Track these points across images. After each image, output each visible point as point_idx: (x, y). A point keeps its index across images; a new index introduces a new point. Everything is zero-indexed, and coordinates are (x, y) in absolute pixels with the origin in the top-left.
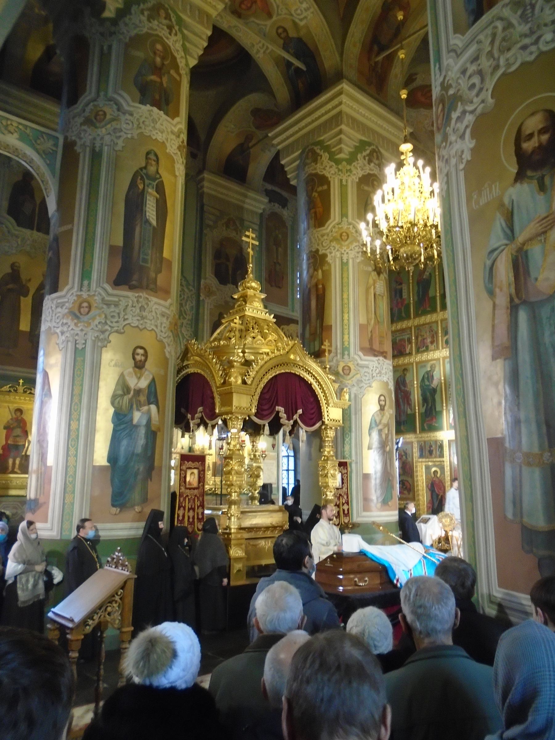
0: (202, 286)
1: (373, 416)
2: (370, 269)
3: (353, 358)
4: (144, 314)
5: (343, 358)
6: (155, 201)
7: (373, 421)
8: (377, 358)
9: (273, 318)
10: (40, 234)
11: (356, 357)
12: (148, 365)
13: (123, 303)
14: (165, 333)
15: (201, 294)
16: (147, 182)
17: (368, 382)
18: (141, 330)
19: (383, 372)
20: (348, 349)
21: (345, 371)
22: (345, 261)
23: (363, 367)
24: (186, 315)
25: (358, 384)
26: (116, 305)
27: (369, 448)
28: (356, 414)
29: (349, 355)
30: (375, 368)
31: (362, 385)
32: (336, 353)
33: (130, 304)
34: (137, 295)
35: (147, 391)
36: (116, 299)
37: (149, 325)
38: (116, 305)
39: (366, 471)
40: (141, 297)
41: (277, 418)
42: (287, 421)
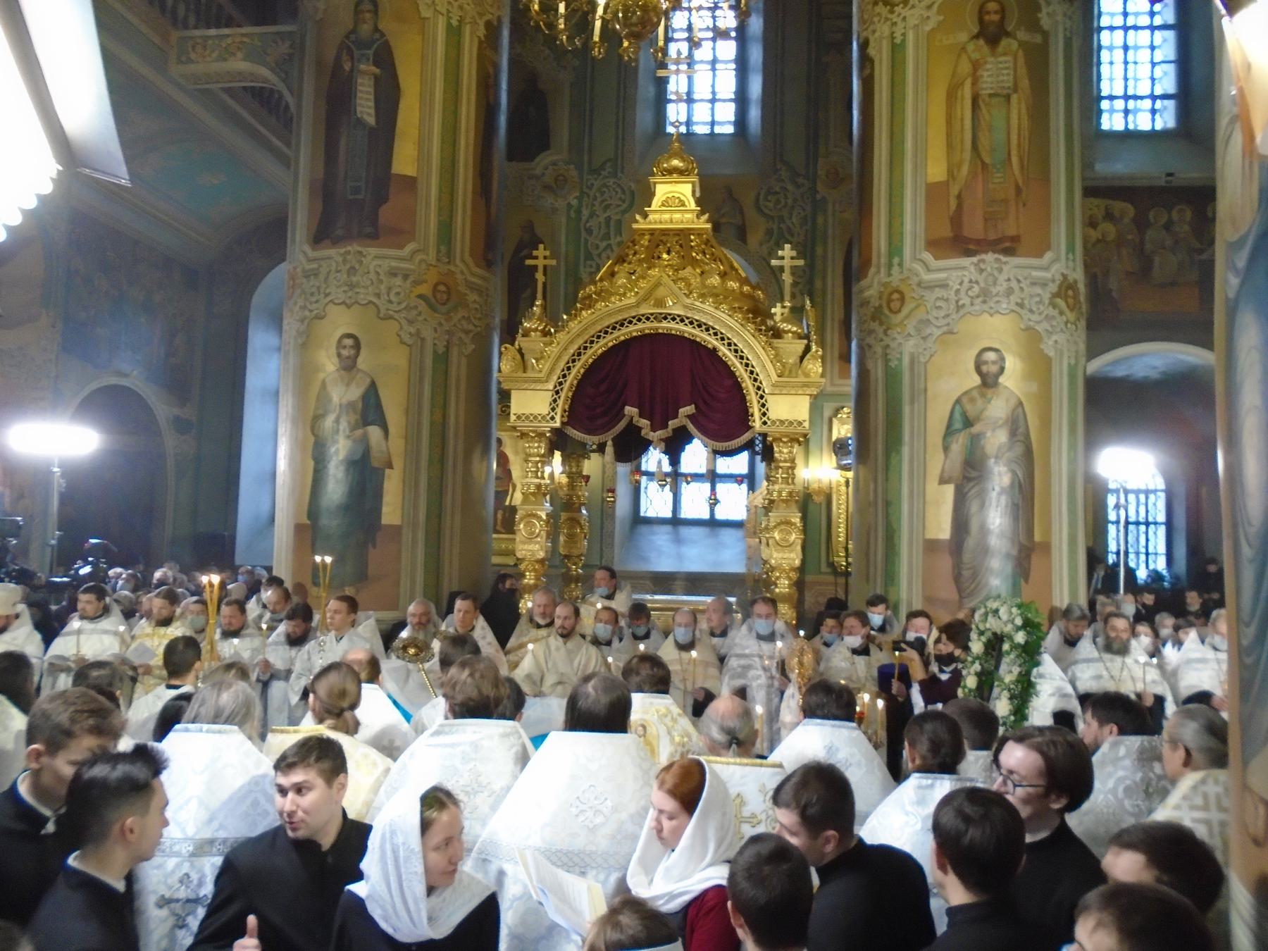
0: (819, 172)
1: (958, 401)
2: (963, 37)
3: (910, 270)
4: (354, 279)
5: (889, 275)
6: (372, 83)
7: (957, 415)
8: (975, 259)
9: (708, 221)
10: (514, 163)
11: (918, 267)
12: (362, 362)
13: (324, 271)
14: (399, 303)
15: (818, 189)
16: (356, 53)
17: (942, 322)
18: (349, 307)
19: (1001, 287)
20: (900, 254)
21: (892, 305)
22: (898, 41)
23: (931, 287)
24: (792, 235)
25: (919, 330)
26: (316, 275)
27: (943, 481)
28: (912, 402)
29: (900, 265)
30: (966, 284)
31: (928, 331)
32: (878, 267)
33: (333, 268)
34: (342, 251)
35: (360, 405)
36: (315, 266)
37: (362, 296)
38: (316, 275)
39: (931, 534)
40: (348, 253)
41: (633, 429)
42: (652, 433)
